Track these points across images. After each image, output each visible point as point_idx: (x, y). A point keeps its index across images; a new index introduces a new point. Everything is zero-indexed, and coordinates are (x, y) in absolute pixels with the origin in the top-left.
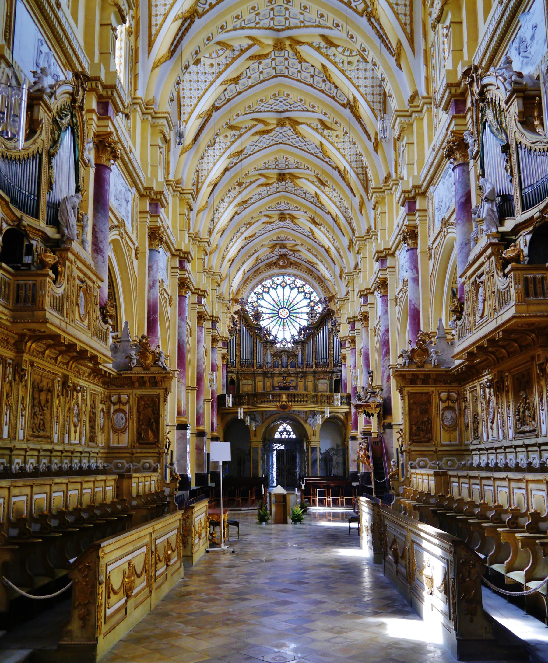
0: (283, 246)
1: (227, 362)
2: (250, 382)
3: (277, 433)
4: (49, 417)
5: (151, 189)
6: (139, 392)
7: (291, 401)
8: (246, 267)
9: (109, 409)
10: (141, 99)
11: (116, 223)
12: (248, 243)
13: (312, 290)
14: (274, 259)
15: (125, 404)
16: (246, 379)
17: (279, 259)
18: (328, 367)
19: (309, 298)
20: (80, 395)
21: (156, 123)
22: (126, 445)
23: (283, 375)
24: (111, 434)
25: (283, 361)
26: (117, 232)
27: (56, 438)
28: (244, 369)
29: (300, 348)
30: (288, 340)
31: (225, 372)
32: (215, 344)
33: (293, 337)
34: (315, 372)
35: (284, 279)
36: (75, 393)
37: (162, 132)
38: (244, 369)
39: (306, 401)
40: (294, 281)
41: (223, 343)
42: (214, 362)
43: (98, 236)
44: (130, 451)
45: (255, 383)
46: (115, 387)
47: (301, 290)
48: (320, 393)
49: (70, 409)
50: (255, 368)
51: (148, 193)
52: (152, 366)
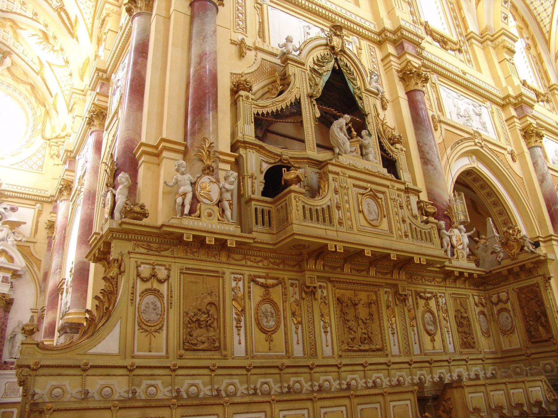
4: (378, 329)
5: (508, 96)
6: (516, 286)
9: (492, 310)
10: (472, 32)
11: (467, 136)
15: (506, 302)
20: (432, 303)
21: (497, 43)
22: (519, 346)
24: (501, 336)
26: (473, 143)
27: (395, 350)
36: (422, 302)
37: (504, 47)
43: (423, 149)
44: (524, 352)
46: (492, 287)
49: (415, 318)
51: (507, 101)
52: (518, 254)
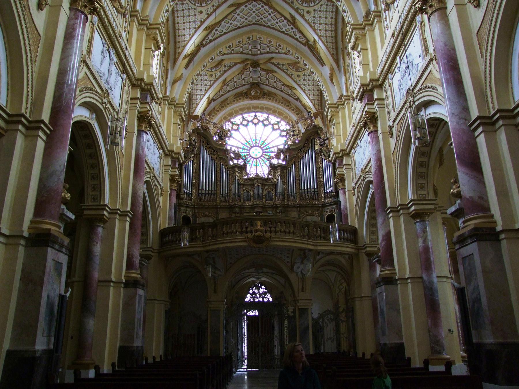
0: (255, 65)
3: (249, 296)
7: (271, 232)
8: (210, 93)
12: (211, 41)
14: (244, 89)
17: (249, 90)
18: (317, 199)
23: (256, 210)
28: (203, 203)
29: (278, 174)
31: (174, 200)
32: (144, 125)
34: (300, 206)
35: (255, 116)
39: (294, 233)
40: (268, 117)
42: (141, 152)
50: (218, 201)
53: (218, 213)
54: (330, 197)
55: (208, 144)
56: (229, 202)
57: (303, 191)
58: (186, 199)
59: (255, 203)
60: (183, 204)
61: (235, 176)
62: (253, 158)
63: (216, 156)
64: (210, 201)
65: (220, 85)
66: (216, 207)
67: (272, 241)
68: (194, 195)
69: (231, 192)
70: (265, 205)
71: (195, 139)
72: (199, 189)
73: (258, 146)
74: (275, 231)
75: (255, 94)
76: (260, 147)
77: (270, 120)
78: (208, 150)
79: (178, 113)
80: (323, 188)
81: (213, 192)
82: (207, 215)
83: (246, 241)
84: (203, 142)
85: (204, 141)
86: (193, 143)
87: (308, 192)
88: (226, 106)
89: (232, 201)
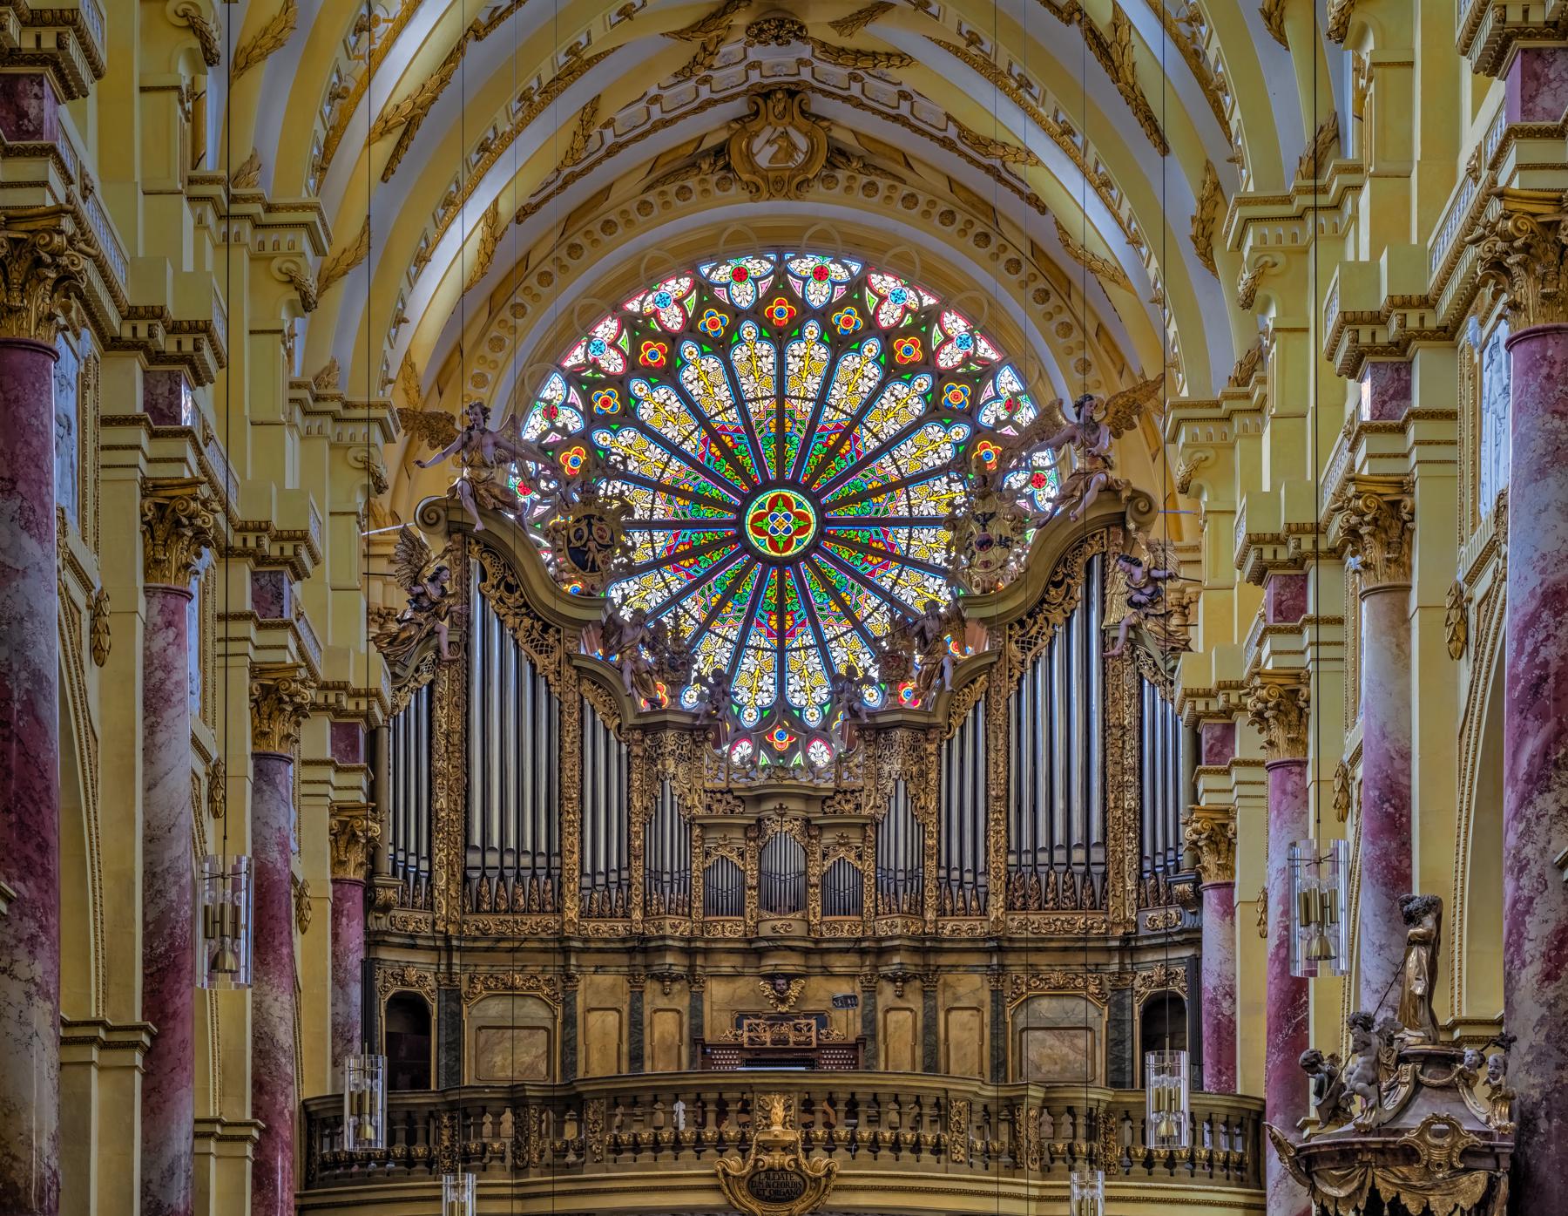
1: (373, 872)
2: (534, 1011)
7: (830, 1148)
13: (985, 349)
16: (511, 991)
18: (1098, 905)
19: (969, 414)
23: (770, 963)
25: (775, 863)
30: (813, 718)
31: (354, 935)
33: (844, 685)
35: (781, 272)
38: (490, 921)
39: (937, 1149)
40: (858, 285)
41: (344, 733)
45: (569, 1021)
47: (907, 350)
48: (1036, 1093)
50: (572, 911)
53: (570, 977)
54: (1169, 902)
55: (510, 589)
56: (627, 915)
57: (1027, 859)
58: (403, 904)
59: (765, 930)
60: (391, 934)
61: (660, 778)
62: (758, 557)
63: (556, 656)
64: (528, 911)
65: (565, 141)
66: (562, 946)
67: (838, 1189)
68: (442, 884)
69: (639, 863)
70: (817, 941)
71: (440, 569)
72: (467, 846)
73: (793, 485)
74: (853, 1139)
75: (773, 158)
76: (804, 489)
77: (871, 301)
78: (510, 621)
79: (351, 453)
80: (1132, 847)
81: (541, 861)
82: (513, 987)
83: (717, 1188)
84: (484, 578)
85: (490, 571)
86: (433, 591)
87: (1051, 864)
88: (595, 242)
89: (645, 914)
